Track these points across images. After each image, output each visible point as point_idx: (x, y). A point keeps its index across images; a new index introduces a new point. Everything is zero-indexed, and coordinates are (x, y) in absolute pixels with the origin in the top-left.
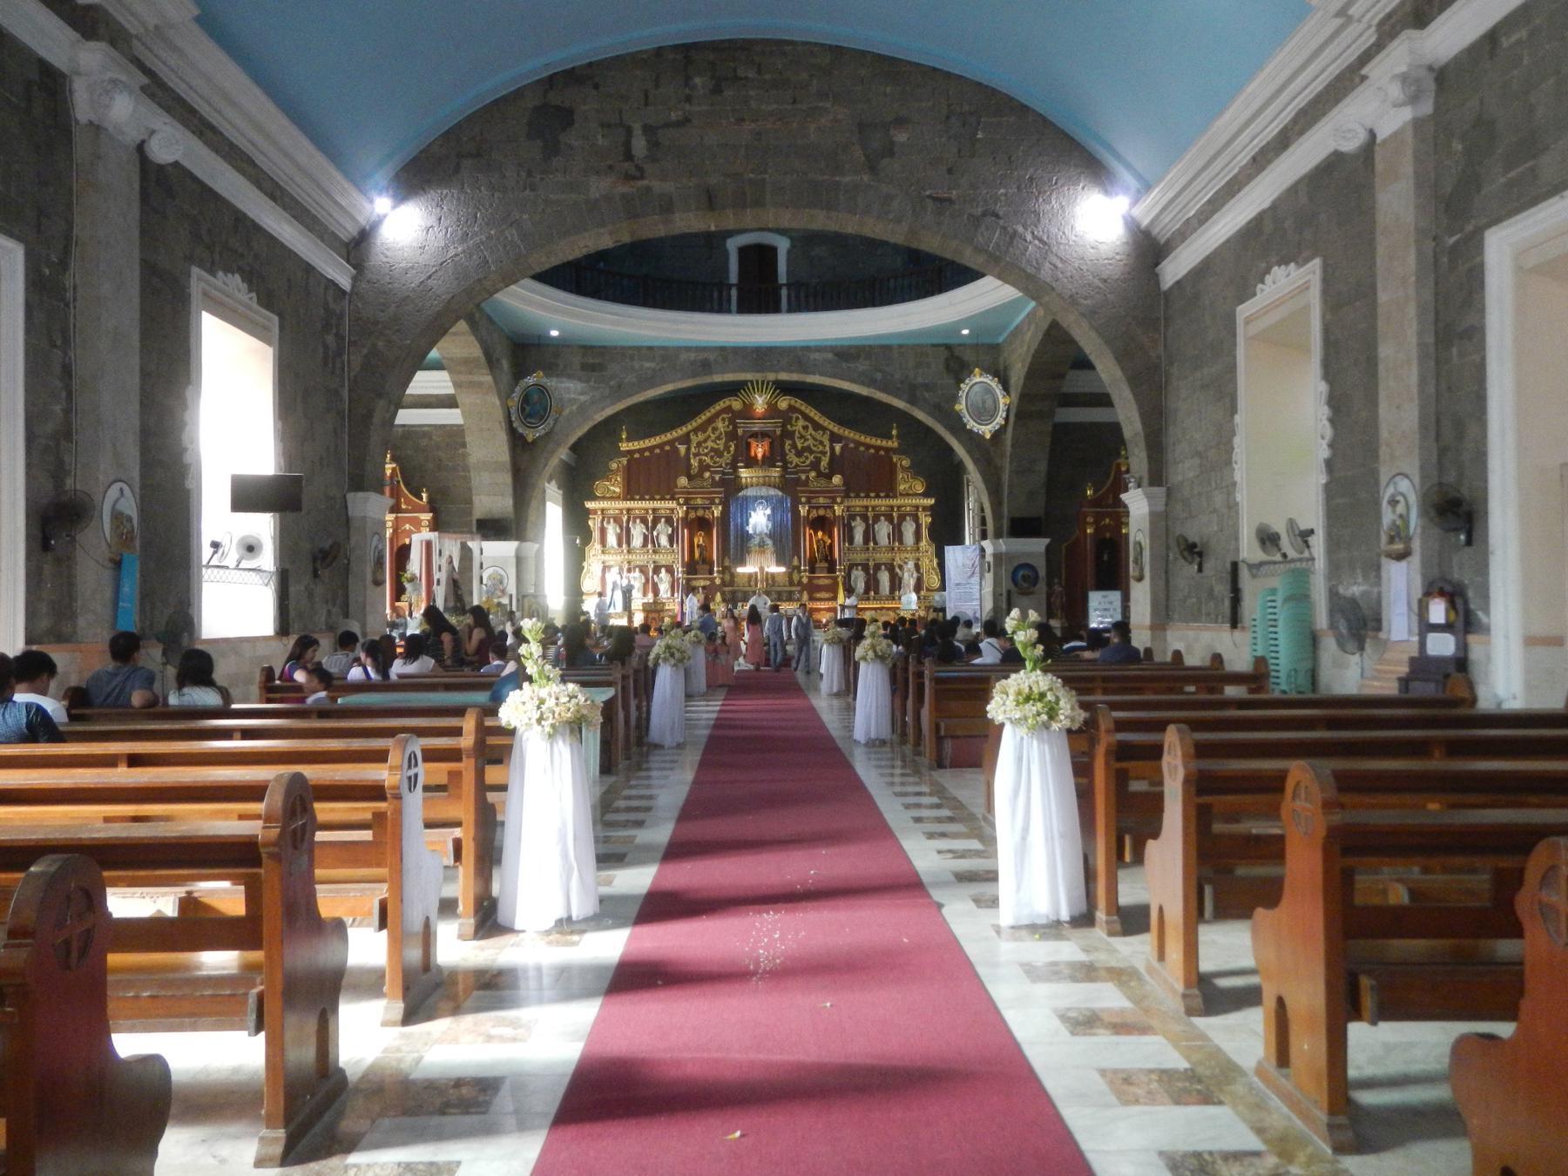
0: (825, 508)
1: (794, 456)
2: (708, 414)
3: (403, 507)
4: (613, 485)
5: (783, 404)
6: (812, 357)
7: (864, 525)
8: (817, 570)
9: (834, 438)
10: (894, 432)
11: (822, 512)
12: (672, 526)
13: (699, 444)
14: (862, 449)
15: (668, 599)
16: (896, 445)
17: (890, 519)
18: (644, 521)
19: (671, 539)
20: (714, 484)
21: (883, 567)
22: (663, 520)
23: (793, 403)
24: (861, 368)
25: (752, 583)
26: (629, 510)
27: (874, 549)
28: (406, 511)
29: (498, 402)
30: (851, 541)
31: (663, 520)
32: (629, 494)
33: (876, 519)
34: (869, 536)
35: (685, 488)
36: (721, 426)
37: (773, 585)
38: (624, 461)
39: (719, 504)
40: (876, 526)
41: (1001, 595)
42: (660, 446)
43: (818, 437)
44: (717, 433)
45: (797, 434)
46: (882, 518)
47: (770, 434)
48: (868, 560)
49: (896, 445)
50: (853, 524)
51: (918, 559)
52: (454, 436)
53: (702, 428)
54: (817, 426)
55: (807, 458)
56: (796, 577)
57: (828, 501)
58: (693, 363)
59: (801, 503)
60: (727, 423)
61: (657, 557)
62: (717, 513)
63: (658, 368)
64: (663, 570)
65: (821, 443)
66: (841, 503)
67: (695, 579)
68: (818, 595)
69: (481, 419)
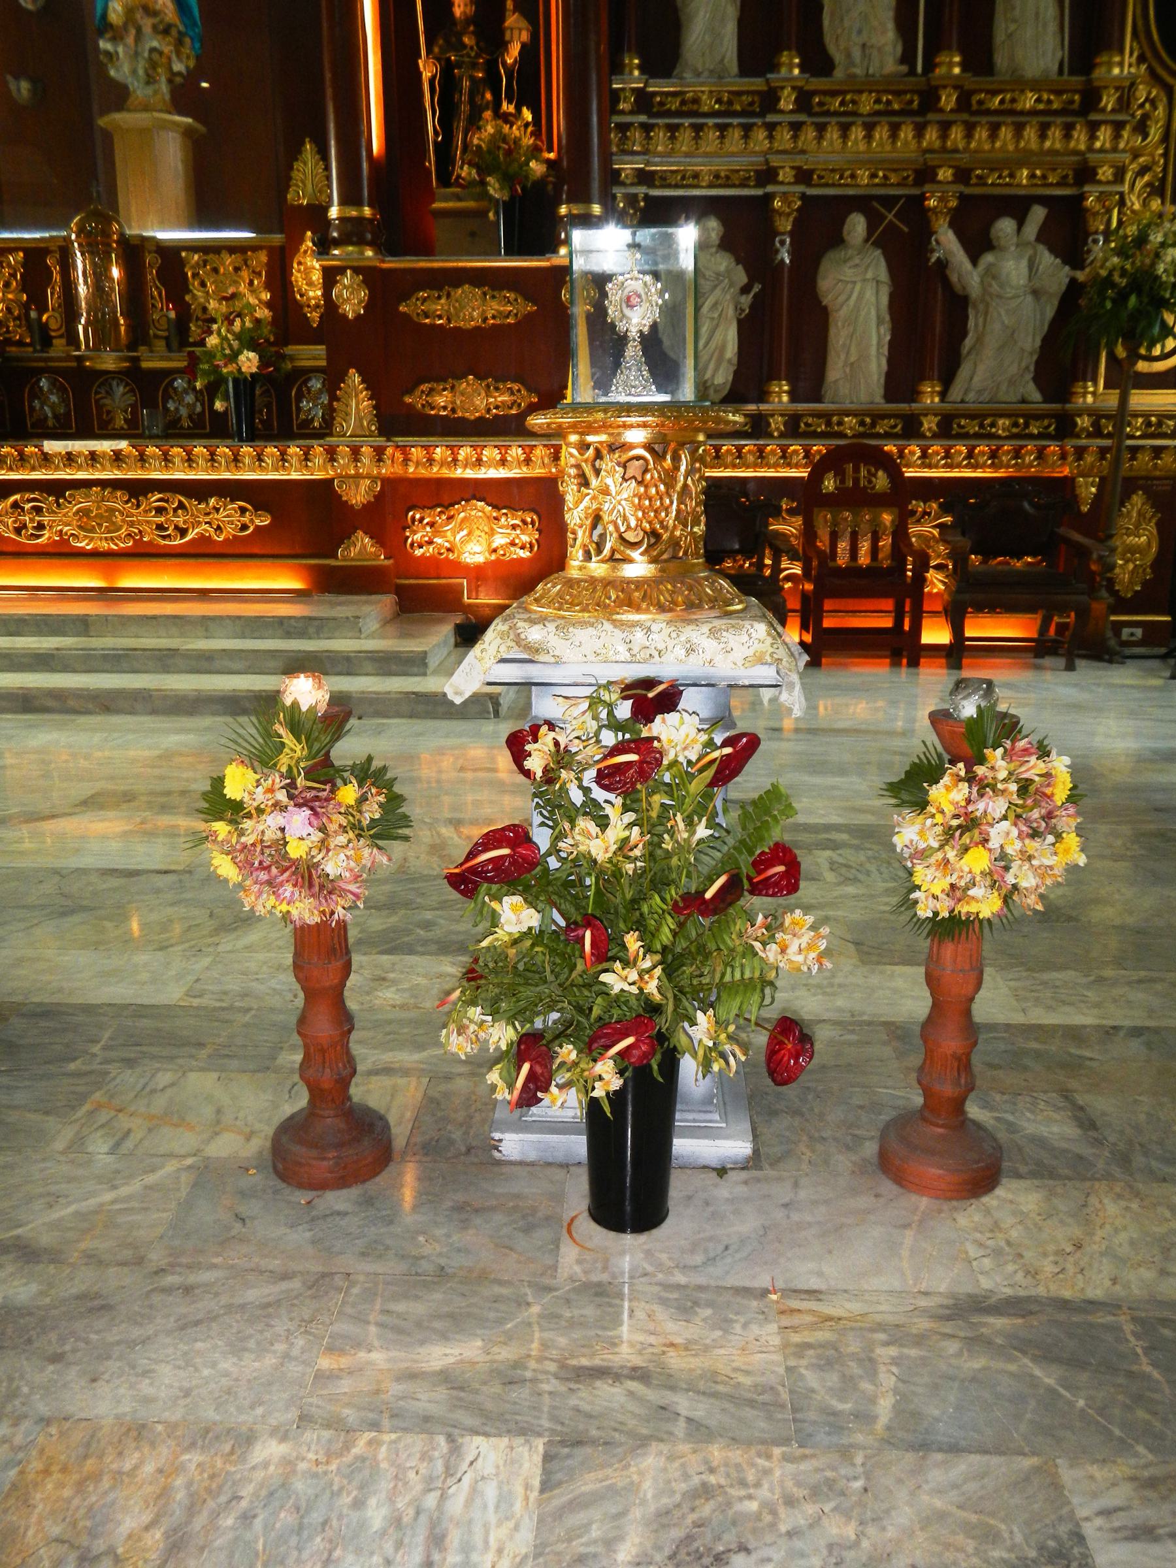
8: (440, 232)
21: (857, 226)
27: (804, 101)
51: (1085, 173)
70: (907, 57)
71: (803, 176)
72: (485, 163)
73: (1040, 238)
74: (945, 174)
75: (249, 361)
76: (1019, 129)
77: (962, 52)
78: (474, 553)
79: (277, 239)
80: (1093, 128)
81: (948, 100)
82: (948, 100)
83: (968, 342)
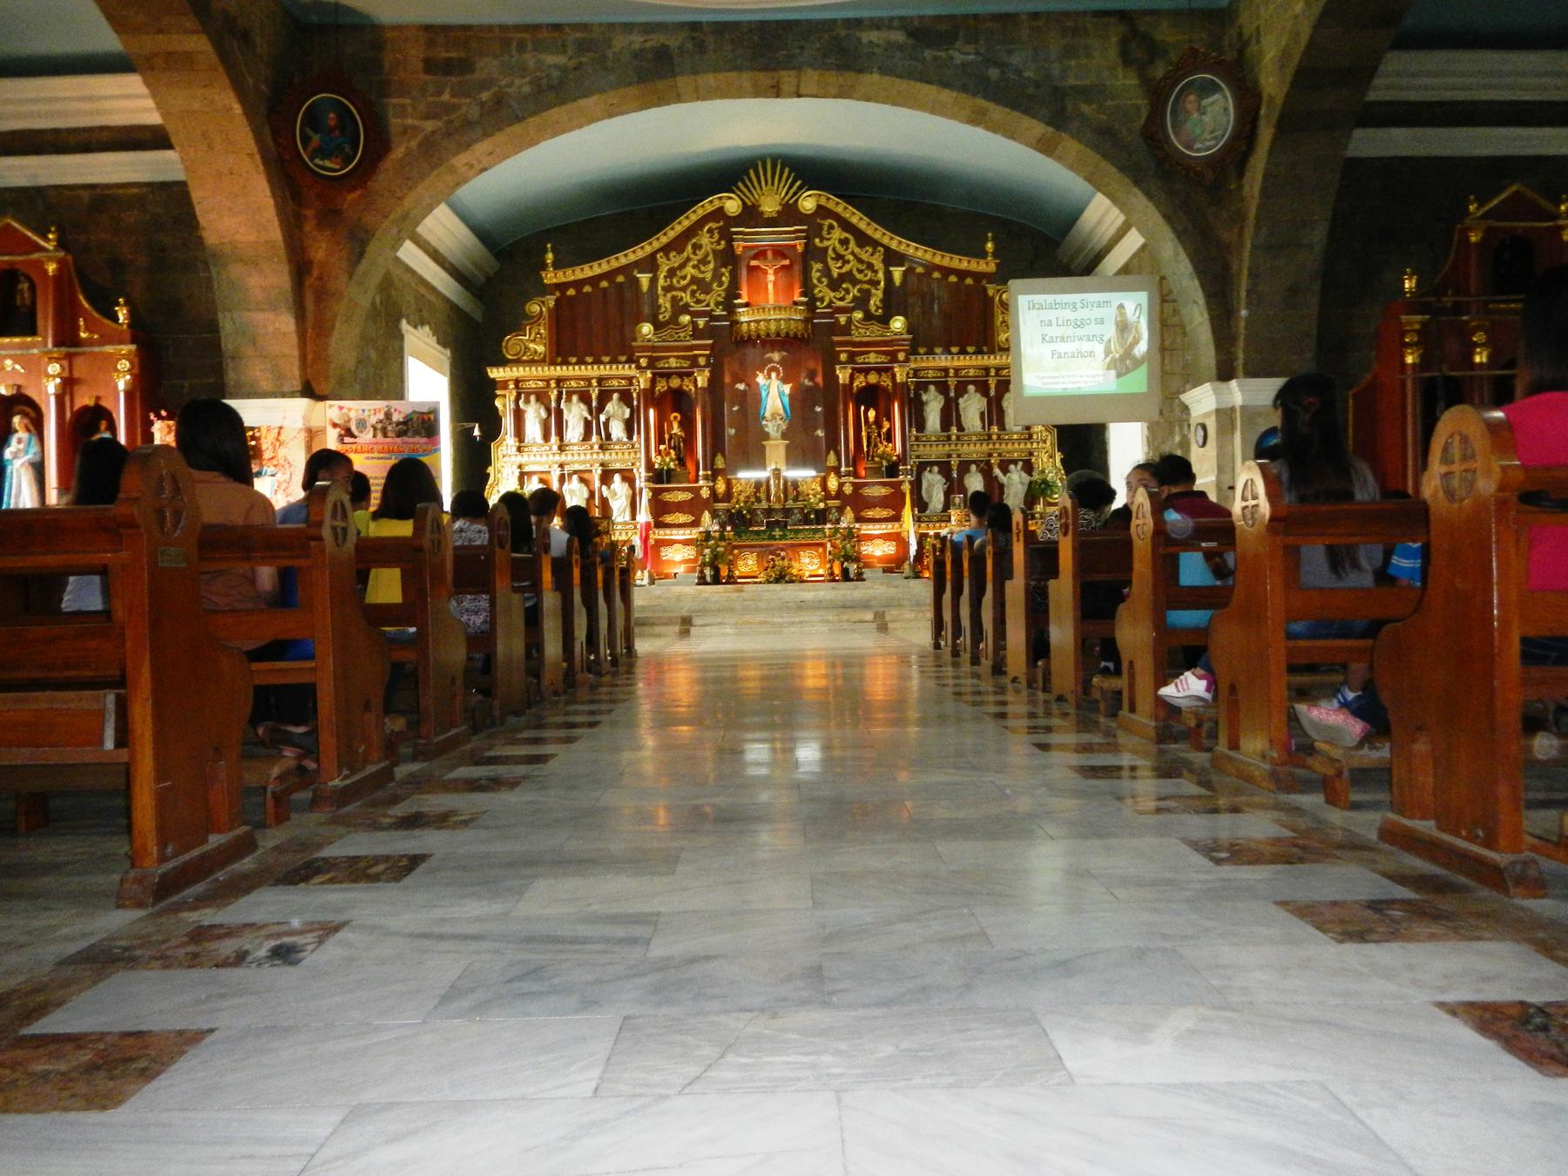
0: (879, 371)
1: (829, 291)
2: (686, 223)
3: (83, 335)
4: (533, 341)
5: (808, 203)
6: (865, 40)
7: (941, 399)
9: (892, 258)
10: (990, 246)
11: (873, 378)
12: (629, 405)
13: (672, 273)
14: (936, 275)
15: (625, 523)
16: (992, 268)
17: (983, 388)
18: (585, 398)
19: (629, 427)
20: (697, 333)
21: (973, 467)
22: (615, 396)
23: (823, 202)
24: (959, 58)
25: (762, 496)
26: (559, 381)
27: (958, 438)
28: (89, 342)
29: (237, 109)
30: (921, 425)
31: (615, 396)
32: (561, 351)
33: (961, 389)
34: (950, 416)
35: (649, 341)
36: (707, 241)
37: (796, 499)
38: (551, 301)
39: (704, 367)
40: (961, 401)
41: (1232, 488)
42: (609, 276)
43: (865, 257)
44: (700, 254)
45: (830, 252)
46: (971, 388)
47: (786, 252)
48: (949, 456)
49: (992, 268)
50: (924, 397)
51: (1031, 454)
52: (175, 196)
53: (676, 245)
54: (863, 239)
55: (847, 291)
56: (833, 483)
57: (883, 358)
58: (637, 55)
59: (841, 363)
60: (716, 236)
61: (606, 457)
62: (702, 379)
63: (572, 63)
64: (617, 477)
65: (870, 266)
66: (907, 360)
67: (668, 490)
68: (870, 514)
69: (210, 147)
70: (984, 428)
71: (959, 456)
72: (882, 457)
73: (1022, 469)
74: (995, 455)
75: (822, 505)
76: (1013, 444)
77: (997, 424)
78: (878, 553)
79: (823, 474)
80: (1032, 443)
81: (994, 437)
82: (994, 437)
83: (1005, 496)
